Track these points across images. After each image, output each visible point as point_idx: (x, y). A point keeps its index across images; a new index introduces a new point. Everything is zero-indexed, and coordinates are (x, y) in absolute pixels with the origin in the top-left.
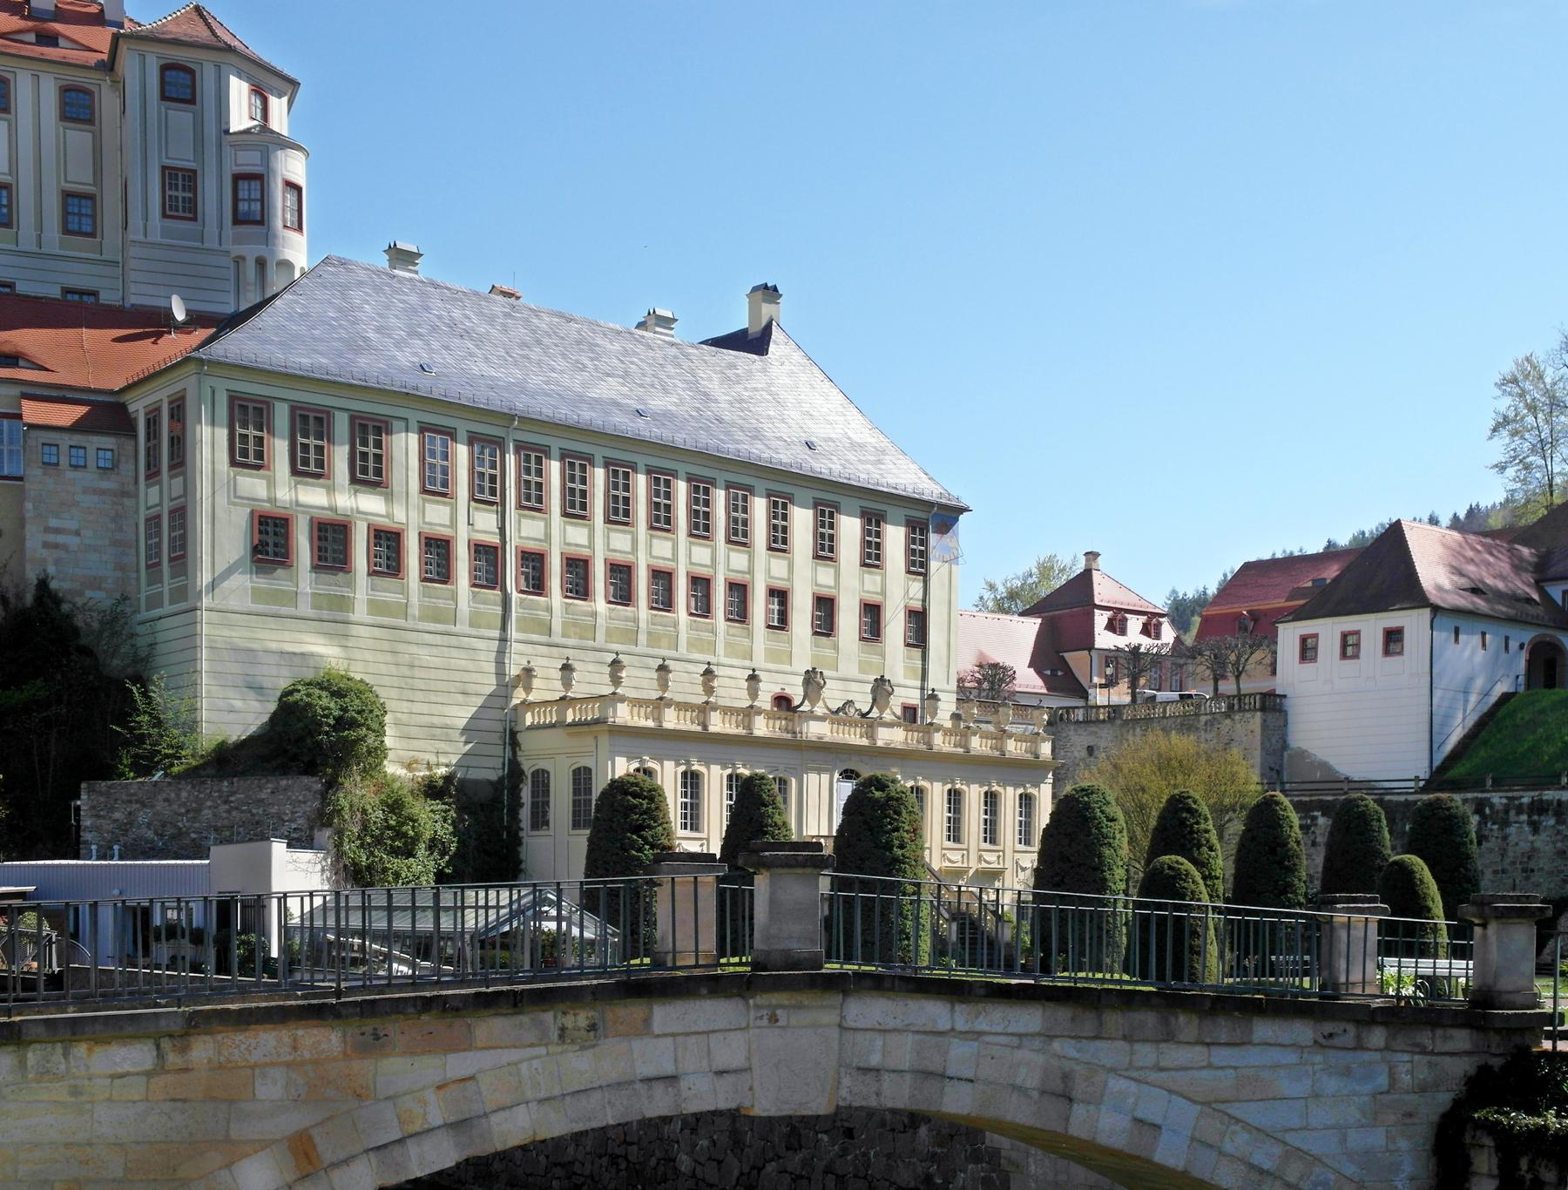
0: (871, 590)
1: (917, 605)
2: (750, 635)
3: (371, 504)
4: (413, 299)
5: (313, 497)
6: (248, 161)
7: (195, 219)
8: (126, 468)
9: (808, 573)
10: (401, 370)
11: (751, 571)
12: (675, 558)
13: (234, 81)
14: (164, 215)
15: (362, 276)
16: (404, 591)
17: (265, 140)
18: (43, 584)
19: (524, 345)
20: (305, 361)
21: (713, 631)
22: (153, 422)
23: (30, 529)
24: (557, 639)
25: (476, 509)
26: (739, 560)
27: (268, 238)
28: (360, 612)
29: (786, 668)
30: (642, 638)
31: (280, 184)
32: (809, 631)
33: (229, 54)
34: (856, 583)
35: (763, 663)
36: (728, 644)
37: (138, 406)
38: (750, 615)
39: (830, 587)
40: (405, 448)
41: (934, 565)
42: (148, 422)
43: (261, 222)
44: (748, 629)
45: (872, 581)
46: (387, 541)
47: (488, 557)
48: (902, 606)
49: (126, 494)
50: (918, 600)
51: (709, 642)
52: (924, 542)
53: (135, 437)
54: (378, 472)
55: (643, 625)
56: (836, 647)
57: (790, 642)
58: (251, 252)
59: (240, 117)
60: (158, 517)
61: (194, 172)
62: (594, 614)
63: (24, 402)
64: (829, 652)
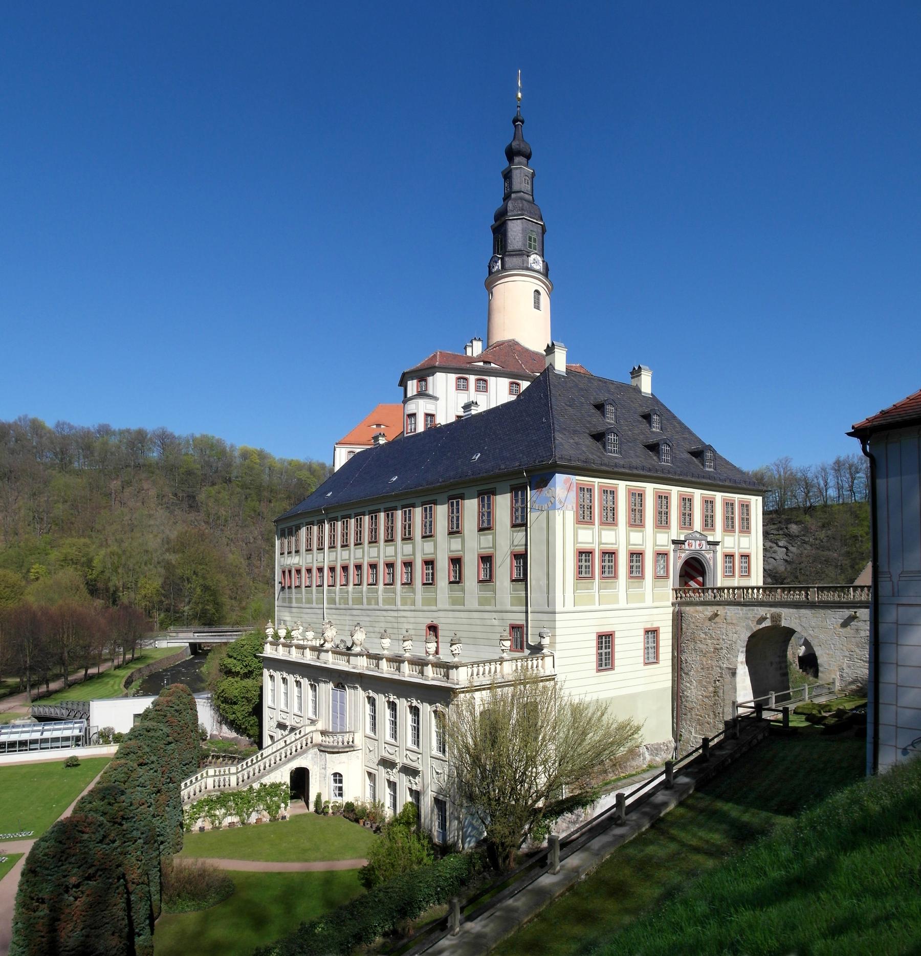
0: (485, 546)
1: (521, 549)
2: (414, 591)
9: (446, 546)
11: (414, 554)
12: (379, 557)
16: (301, 593)
21: (394, 592)
24: (338, 606)
25: (319, 553)
26: (408, 548)
28: (294, 604)
29: (434, 608)
30: (365, 600)
32: (447, 582)
34: (475, 545)
35: (421, 607)
36: (402, 598)
38: (413, 580)
39: (459, 551)
41: (532, 517)
44: (413, 588)
45: (486, 540)
48: (509, 553)
50: (522, 545)
51: (392, 598)
52: (525, 501)
55: (364, 594)
56: (463, 590)
57: (436, 592)
62: (347, 592)
64: (459, 594)
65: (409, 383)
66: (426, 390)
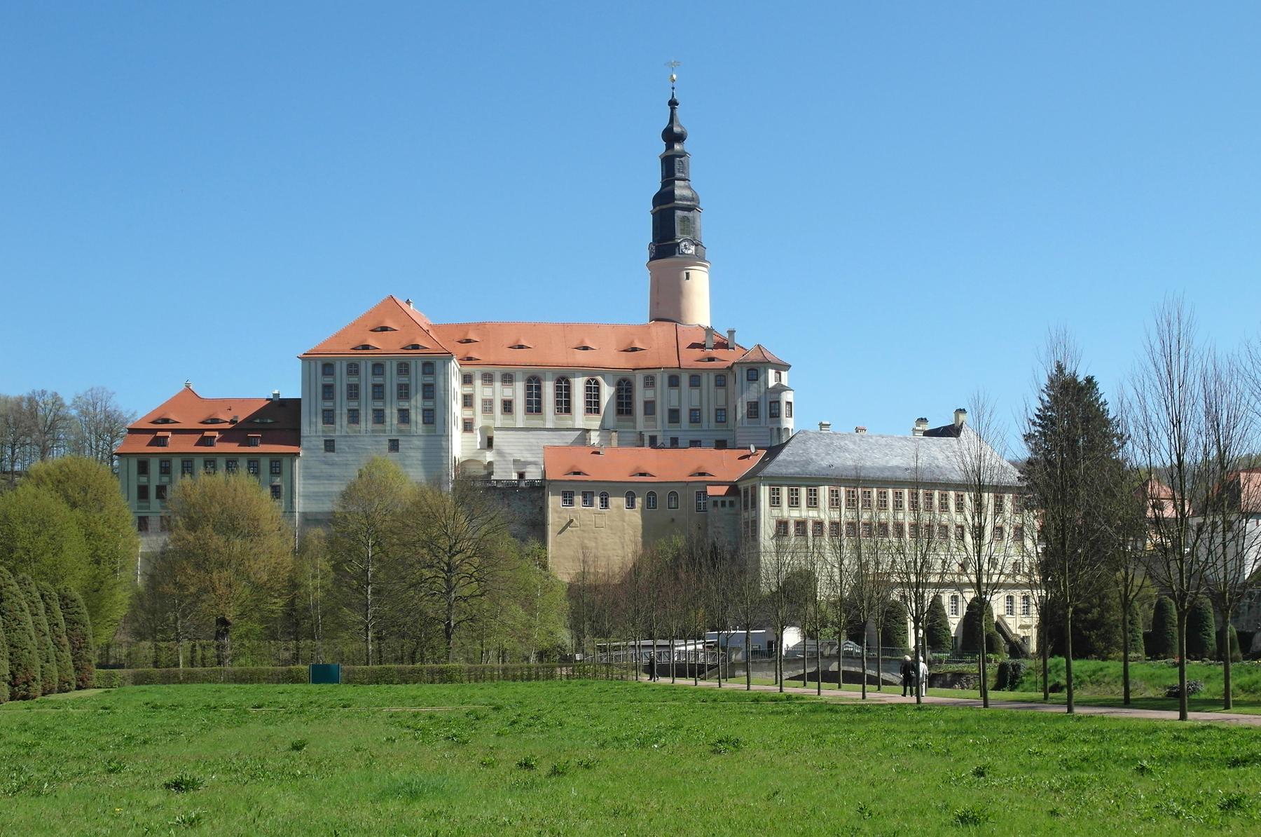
3: (813, 514)
4: (828, 441)
5: (795, 514)
6: (773, 397)
7: (758, 417)
8: (737, 506)
10: (823, 468)
13: (770, 371)
14: (748, 418)
15: (811, 435)
17: (780, 389)
18: (714, 544)
19: (866, 450)
20: (792, 471)
22: (746, 492)
23: (709, 528)
27: (779, 422)
31: (785, 403)
33: (766, 364)
37: (742, 486)
40: (824, 492)
42: (744, 492)
43: (779, 417)
46: (819, 524)
47: (852, 526)
49: (737, 514)
53: (740, 496)
54: (815, 503)
58: (775, 426)
59: (772, 383)
60: (748, 522)
61: (757, 402)
63: (708, 487)
65: (770, 371)
66: (780, 381)
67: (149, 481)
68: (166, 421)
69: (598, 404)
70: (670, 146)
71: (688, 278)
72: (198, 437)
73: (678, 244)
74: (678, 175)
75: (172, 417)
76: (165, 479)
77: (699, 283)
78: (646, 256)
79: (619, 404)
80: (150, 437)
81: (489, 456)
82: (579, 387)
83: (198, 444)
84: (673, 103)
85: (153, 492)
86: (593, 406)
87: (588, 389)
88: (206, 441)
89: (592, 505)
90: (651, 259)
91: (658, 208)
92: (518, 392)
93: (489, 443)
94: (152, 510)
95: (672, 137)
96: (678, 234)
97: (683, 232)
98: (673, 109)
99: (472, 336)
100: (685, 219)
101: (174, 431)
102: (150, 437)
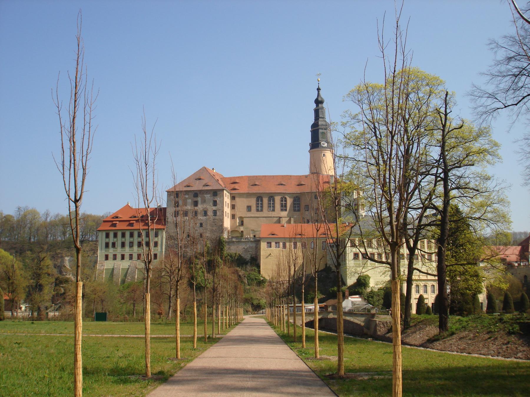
67: (109, 240)
68: (117, 217)
69: (286, 206)
70: (317, 106)
71: (324, 156)
72: (128, 223)
73: (320, 143)
74: (320, 116)
75: (120, 216)
76: (115, 240)
77: (328, 158)
78: (309, 148)
79: (294, 207)
80: (110, 224)
81: (242, 229)
82: (278, 199)
83: (128, 226)
84: (318, 89)
85: (110, 245)
86: (284, 207)
87: (282, 201)
88: (131, 225)
89: (279, 247)
90: (310, 149)
91: (313, 129)
92: (253, 202)
93: (242, 223)
94: (134, 251)
95: (318, 102)
96: (320, 139)
97: (323, 138)
98: (318, 92)
99: (237, 181)
100: (323, 133)
101: (120, 221)
102: (128, 223)
